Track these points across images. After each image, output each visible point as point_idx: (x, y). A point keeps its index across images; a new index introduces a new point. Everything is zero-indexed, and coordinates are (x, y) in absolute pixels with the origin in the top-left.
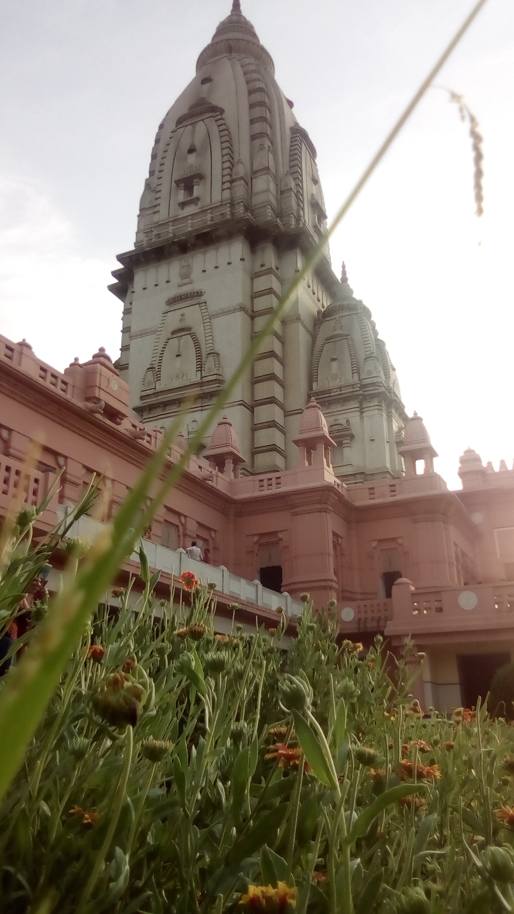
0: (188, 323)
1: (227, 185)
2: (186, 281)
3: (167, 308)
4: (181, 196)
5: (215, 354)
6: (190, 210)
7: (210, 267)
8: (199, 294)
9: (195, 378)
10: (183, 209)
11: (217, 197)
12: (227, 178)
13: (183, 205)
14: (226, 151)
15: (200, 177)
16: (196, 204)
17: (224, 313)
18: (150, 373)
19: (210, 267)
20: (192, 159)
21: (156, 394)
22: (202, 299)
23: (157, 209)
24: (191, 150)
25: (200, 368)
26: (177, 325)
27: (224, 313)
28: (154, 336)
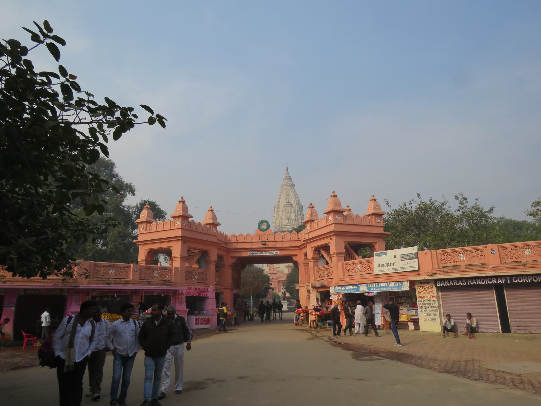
4: (287, 221)
6: (289, 224)
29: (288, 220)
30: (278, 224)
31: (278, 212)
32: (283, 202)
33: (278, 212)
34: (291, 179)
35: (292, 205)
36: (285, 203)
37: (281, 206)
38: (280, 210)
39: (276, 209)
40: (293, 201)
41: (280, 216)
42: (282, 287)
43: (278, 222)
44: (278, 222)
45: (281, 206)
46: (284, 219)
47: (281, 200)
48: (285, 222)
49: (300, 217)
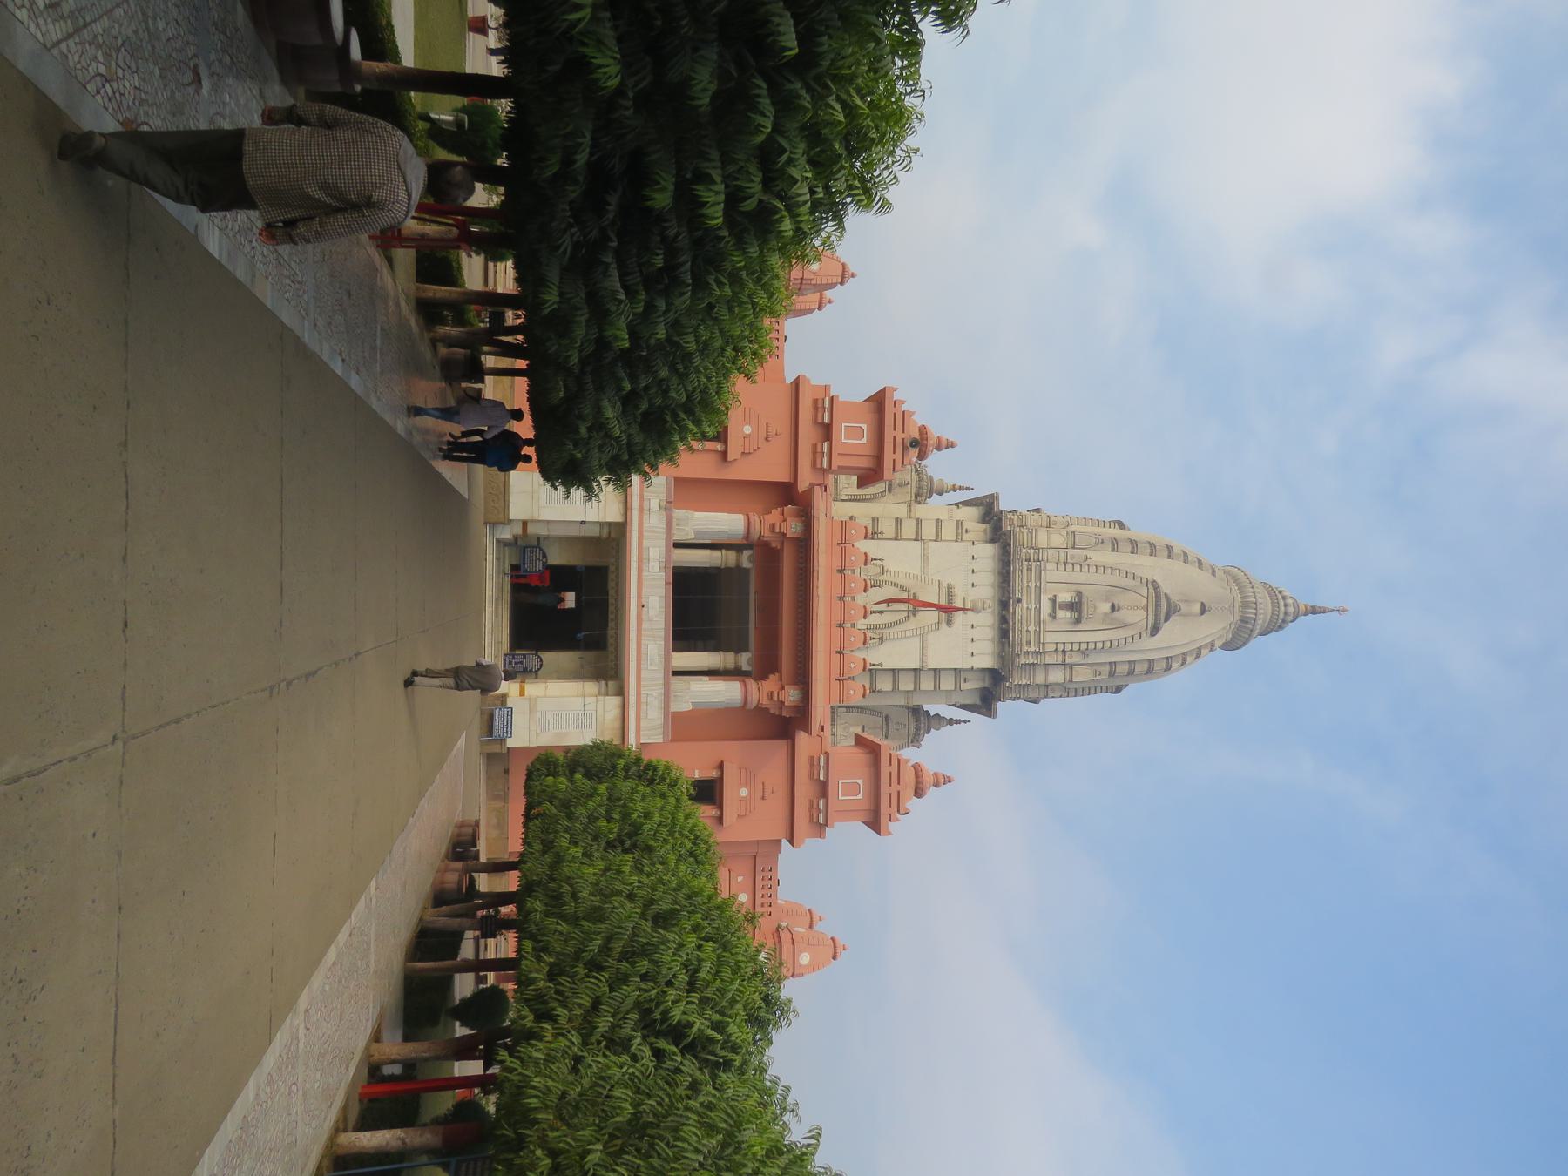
1: (1061, 647)
4: (1065, 597)
5: (881, 640)
6: (1046, 608)
7: (975, 634)
11: (1050, 638)
12: (1068, 647)
13: (1053, 601)
14: (1100, 645)
15: (1078, 621)
18: (879, 570)
19: (975, 634)
20: (1106, 607)
22: (944, 625)
23: (1062, 567)
24: (1113, 608)
28: (917, 572)
29: (1075, 606)
30: (1042, 539)
31: (1115, 544)
32: (1173, 578)
33: (1115, 544)
34: (1262, 634)
35: (1155, 630)
36: (1165, 588)
37: (1146, 566)
38: (1123, 559)
39: (1116, 532)
40: (1174, 635)
41: (1098, 557)
42: (728, 522)
43: (1058, 540)
44: (1058, 540)
45: (1146, 566)
47: (1177, 565)
48: (1059, 584)
49: (1082, 676)
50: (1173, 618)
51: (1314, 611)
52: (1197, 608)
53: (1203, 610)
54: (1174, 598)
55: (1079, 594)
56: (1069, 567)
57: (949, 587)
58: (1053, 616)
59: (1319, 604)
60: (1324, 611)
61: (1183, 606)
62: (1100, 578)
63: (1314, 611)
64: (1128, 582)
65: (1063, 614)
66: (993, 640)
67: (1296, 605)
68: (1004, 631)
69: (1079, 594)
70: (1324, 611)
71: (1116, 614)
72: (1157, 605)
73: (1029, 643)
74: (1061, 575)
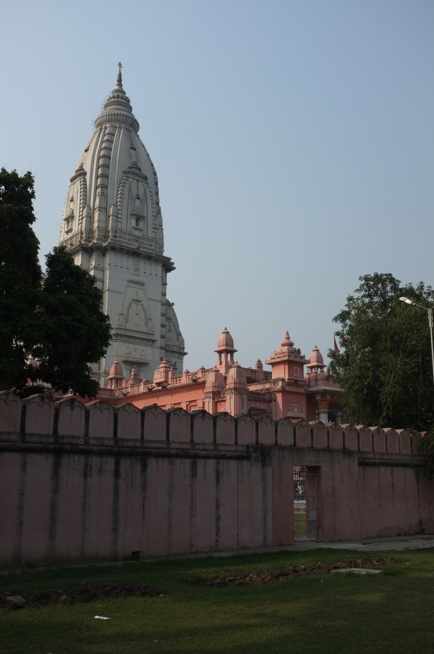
0: (140, 299)
1: (154, 230)
2: (136, 273)
3: (127, 284)
4: (133, 222)
6: (137, 233)
8: (143, 284)
9: (145, 331)
10: (134, 230)
11: (151, 235)
15: (144, 218)
16: (141, 232)
17: (155, 300)
18: (122, 317)
20: (138, 202)
21: (125, 330)
22: (144, 287)
23: (120, 220)
24: (139, 198)
25: (146, 325)
26: (135, 298)
27: (155, 300)
29: (139, 218)
36: (126, 168)
46: (124, 212)
50: (139, 166)
51: (120, 80)
52: (133, 152)
53: (134, 149)
54: (130, 165)
55: (132, 215)
56: (119, 216)
57: (130, 281)
58: (140, 230)
59: (116, 78)
60: (120, 75)
61: (135, 160)
62: (125, 201)
63: (120, 80)
64: (127, 186)
65: (141, 223)
66: (151, 264)
67: (116, 91)
68: (149, 258)
69: (132, 215)
70: (120, 75)
71: (141, 198)
72: (136, 174)
73: (151, 245)
74: (124, 220)
